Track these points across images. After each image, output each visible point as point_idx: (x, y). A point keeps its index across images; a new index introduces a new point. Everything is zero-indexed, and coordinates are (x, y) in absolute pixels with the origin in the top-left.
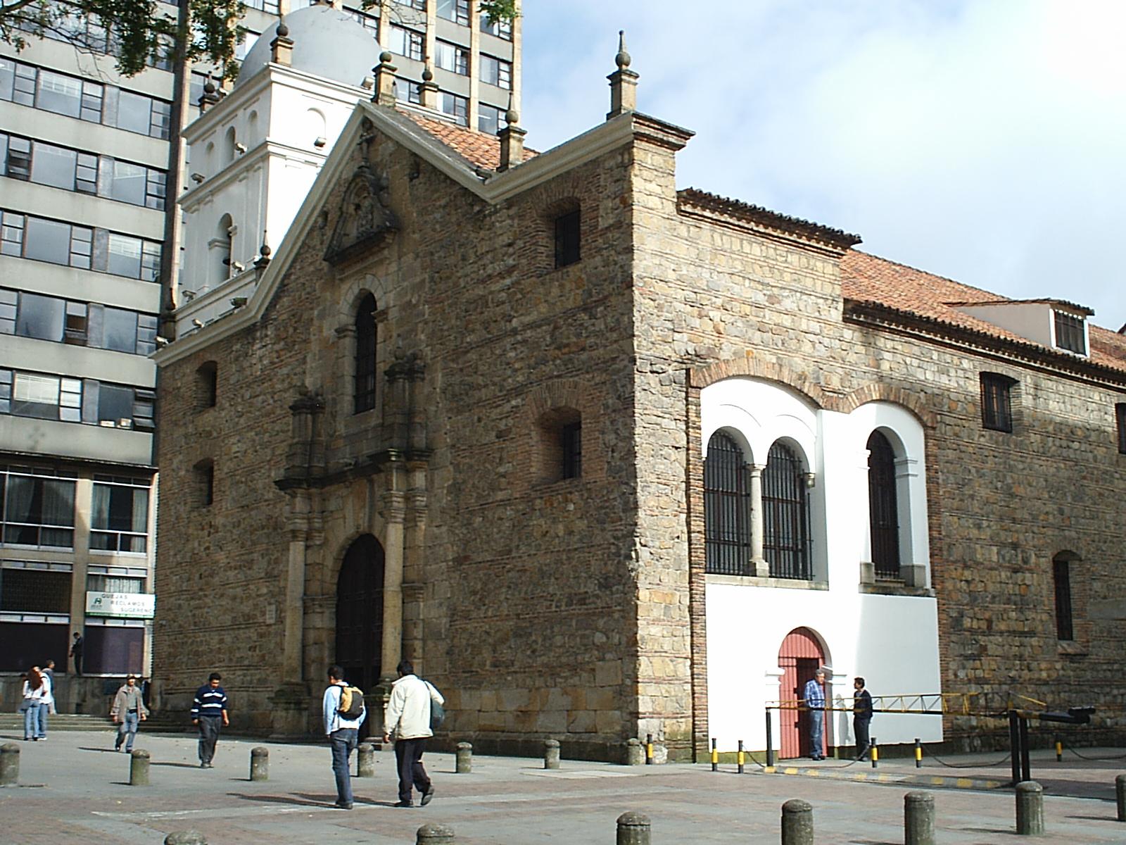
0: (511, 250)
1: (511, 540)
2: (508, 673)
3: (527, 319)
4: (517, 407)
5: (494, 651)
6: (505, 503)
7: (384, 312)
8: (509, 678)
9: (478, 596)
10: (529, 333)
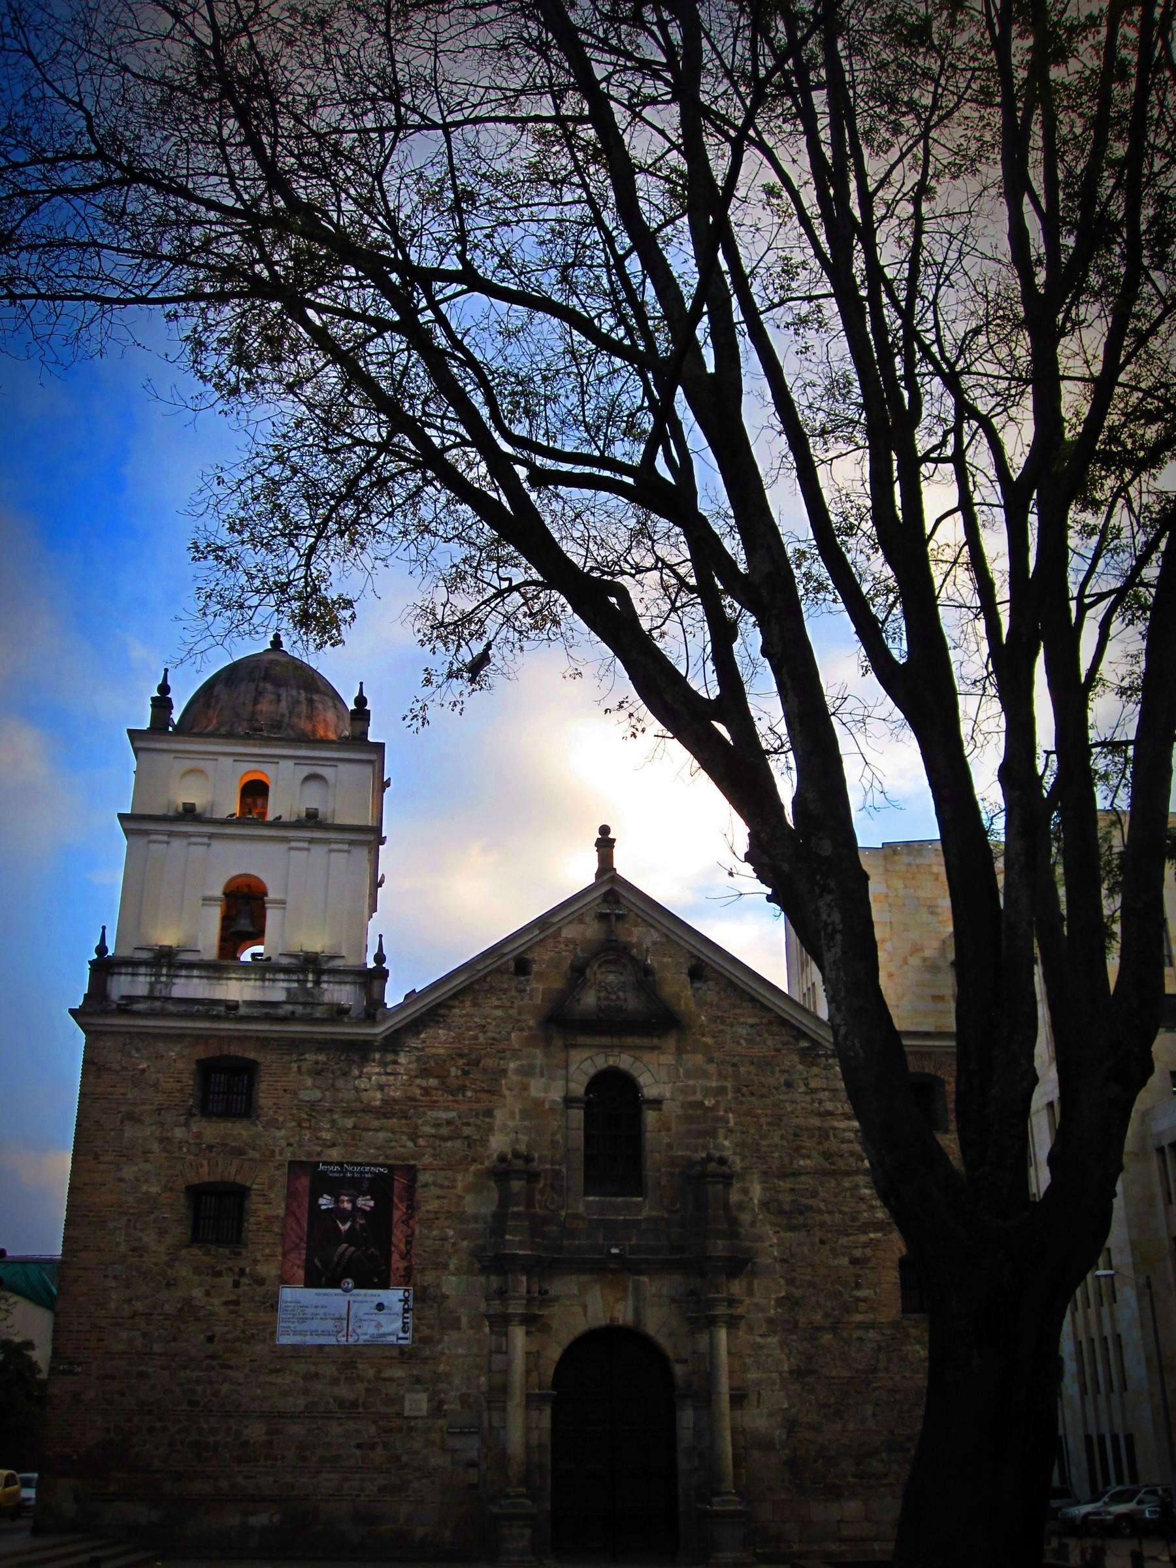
1: (878, 1361)
4: (878, 1240)
6: (866, 1326)
7: (657, 1103)
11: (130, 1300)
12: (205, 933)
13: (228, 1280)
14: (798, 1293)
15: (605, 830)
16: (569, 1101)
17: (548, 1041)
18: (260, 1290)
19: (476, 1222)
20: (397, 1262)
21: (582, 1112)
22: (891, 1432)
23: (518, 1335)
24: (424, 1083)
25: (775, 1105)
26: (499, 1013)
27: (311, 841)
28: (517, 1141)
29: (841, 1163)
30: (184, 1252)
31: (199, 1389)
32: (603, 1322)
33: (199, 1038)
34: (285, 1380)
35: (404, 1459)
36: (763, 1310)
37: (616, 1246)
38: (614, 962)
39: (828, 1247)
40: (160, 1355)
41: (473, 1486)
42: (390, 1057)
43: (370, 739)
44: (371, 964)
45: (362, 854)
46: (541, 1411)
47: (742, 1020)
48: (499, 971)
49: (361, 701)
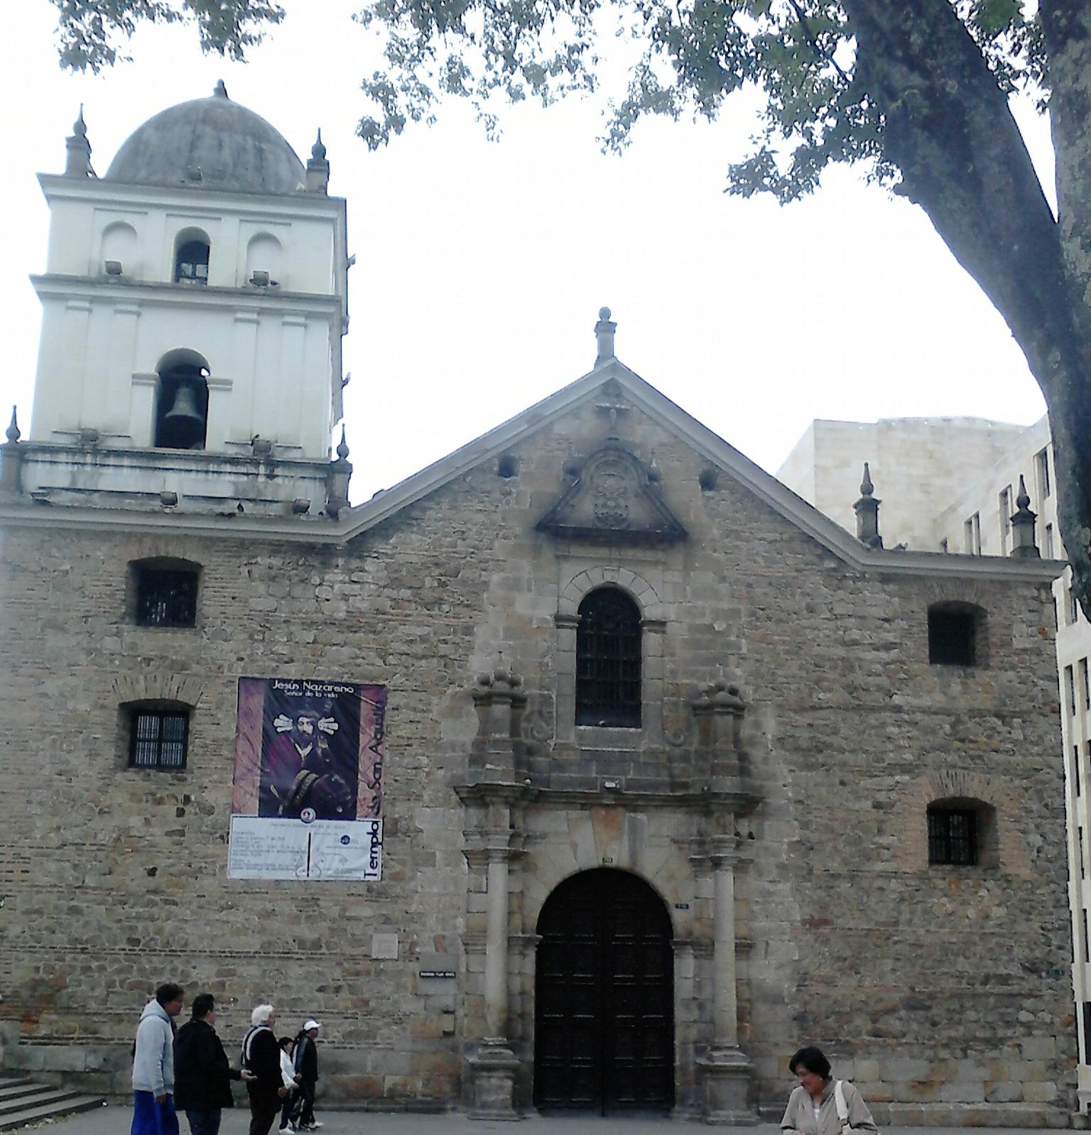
0: (886, 625)
1: (900, 913)
2: (900, 1045)
3: (916, 702)
5: (874, 1021)
7: (660, 625)
8: (899, 1049)
9: (847, 963)
10: (918, 716)
11: (59, 828)
12: (136, 416)
13: (170, 809)
14: (814, 837)
15: (605, 313)
16: (560, 619)
17: (536, 551)
18: (209, 820)
19: (454, 751)
20: (364, 792)
21: (575, 632)
22: (913, 989)
23: (498, 871)
24: (394, 594)
25: (796, 632)
26: (480, 518)
27: (261, 312)
28: (501, 660)
29: (867, 699)
30: (119, 776)
31: (140, 926)
32: (595, 862)
33: (131, 536)
34: (237, 918)
35: (372, 1004)
36: (775, 855)
37: (612, 780)
38: (614, 464)
39: (847, 789)
40: (94, 889)
41: (447, 1034)
42: (355, 563)
43: (330, 193)
44: (335, 457)
45: (321, 332)
46: (523, 955)
47: (761, 535)
48: (480, 469)
49: (319, 151)
